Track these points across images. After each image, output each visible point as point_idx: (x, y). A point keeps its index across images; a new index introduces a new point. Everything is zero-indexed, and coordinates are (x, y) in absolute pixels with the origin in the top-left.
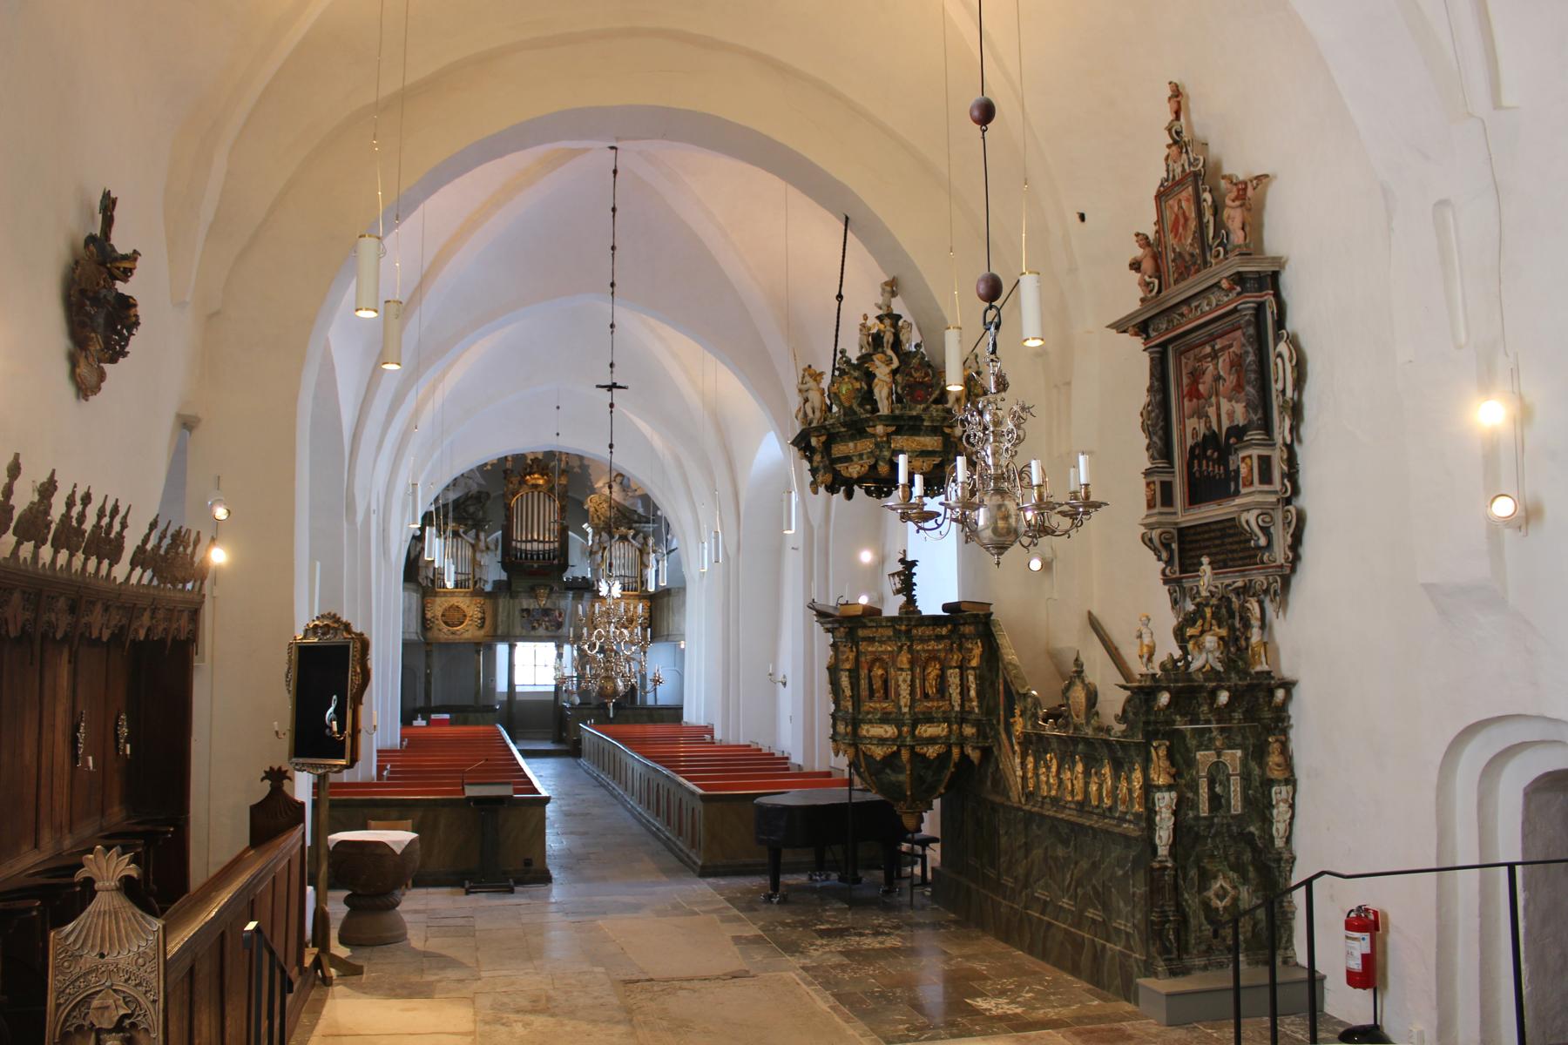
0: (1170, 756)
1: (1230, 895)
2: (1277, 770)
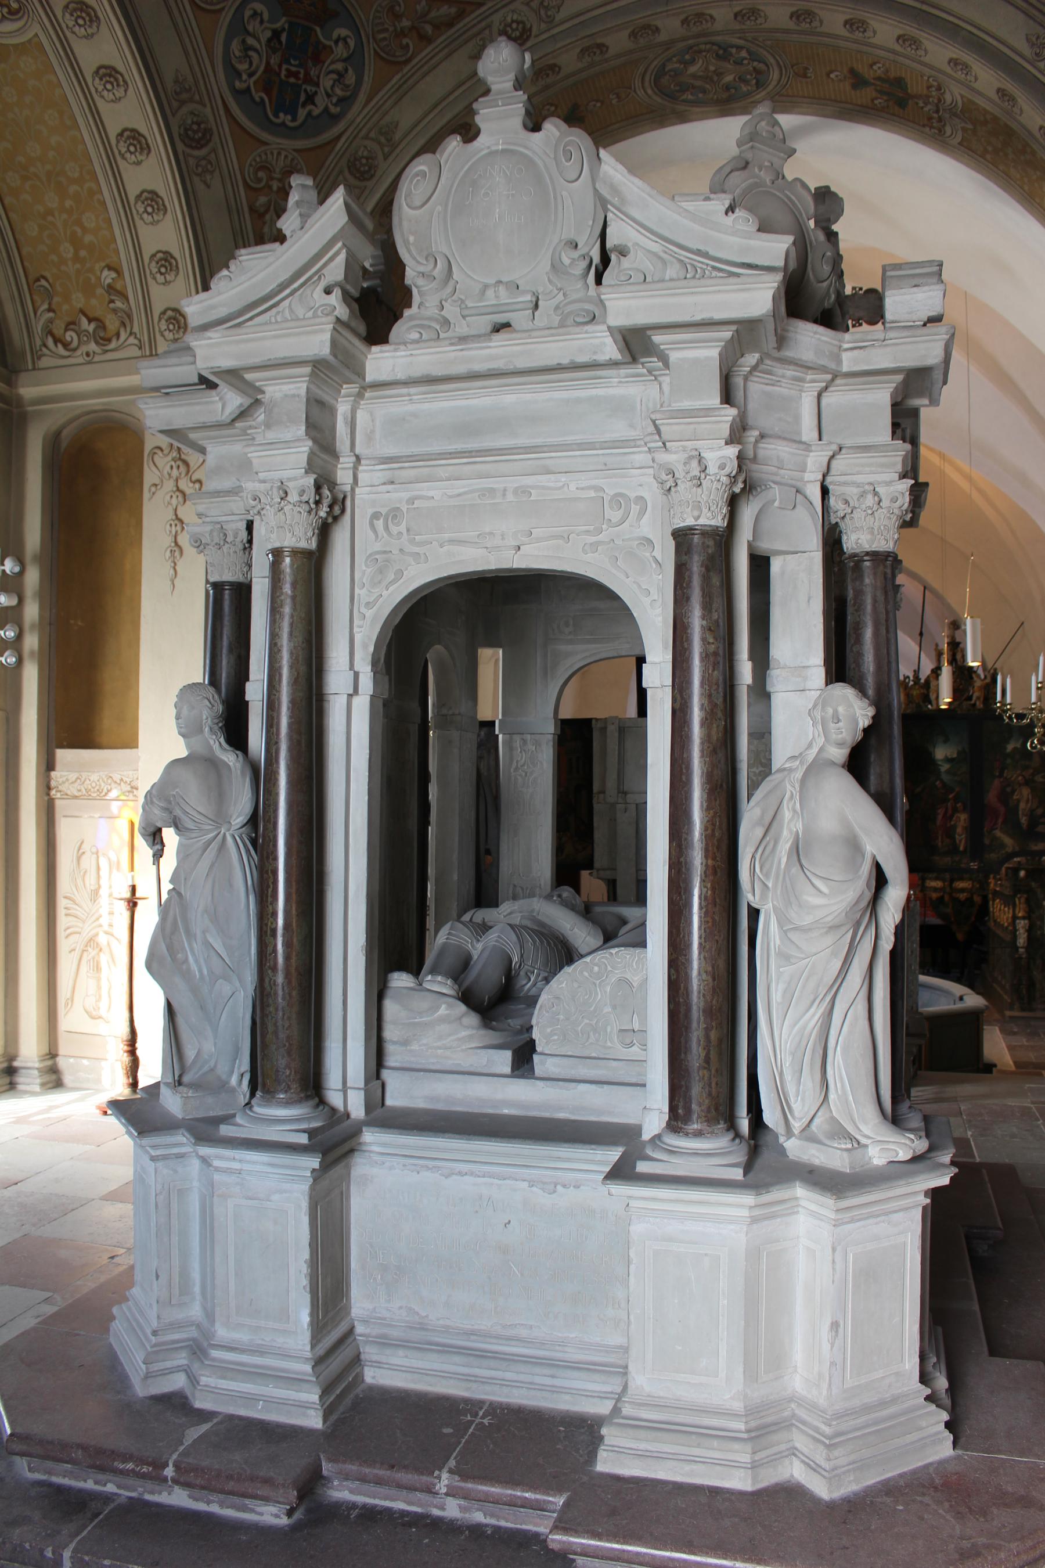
0: (1027, 901)
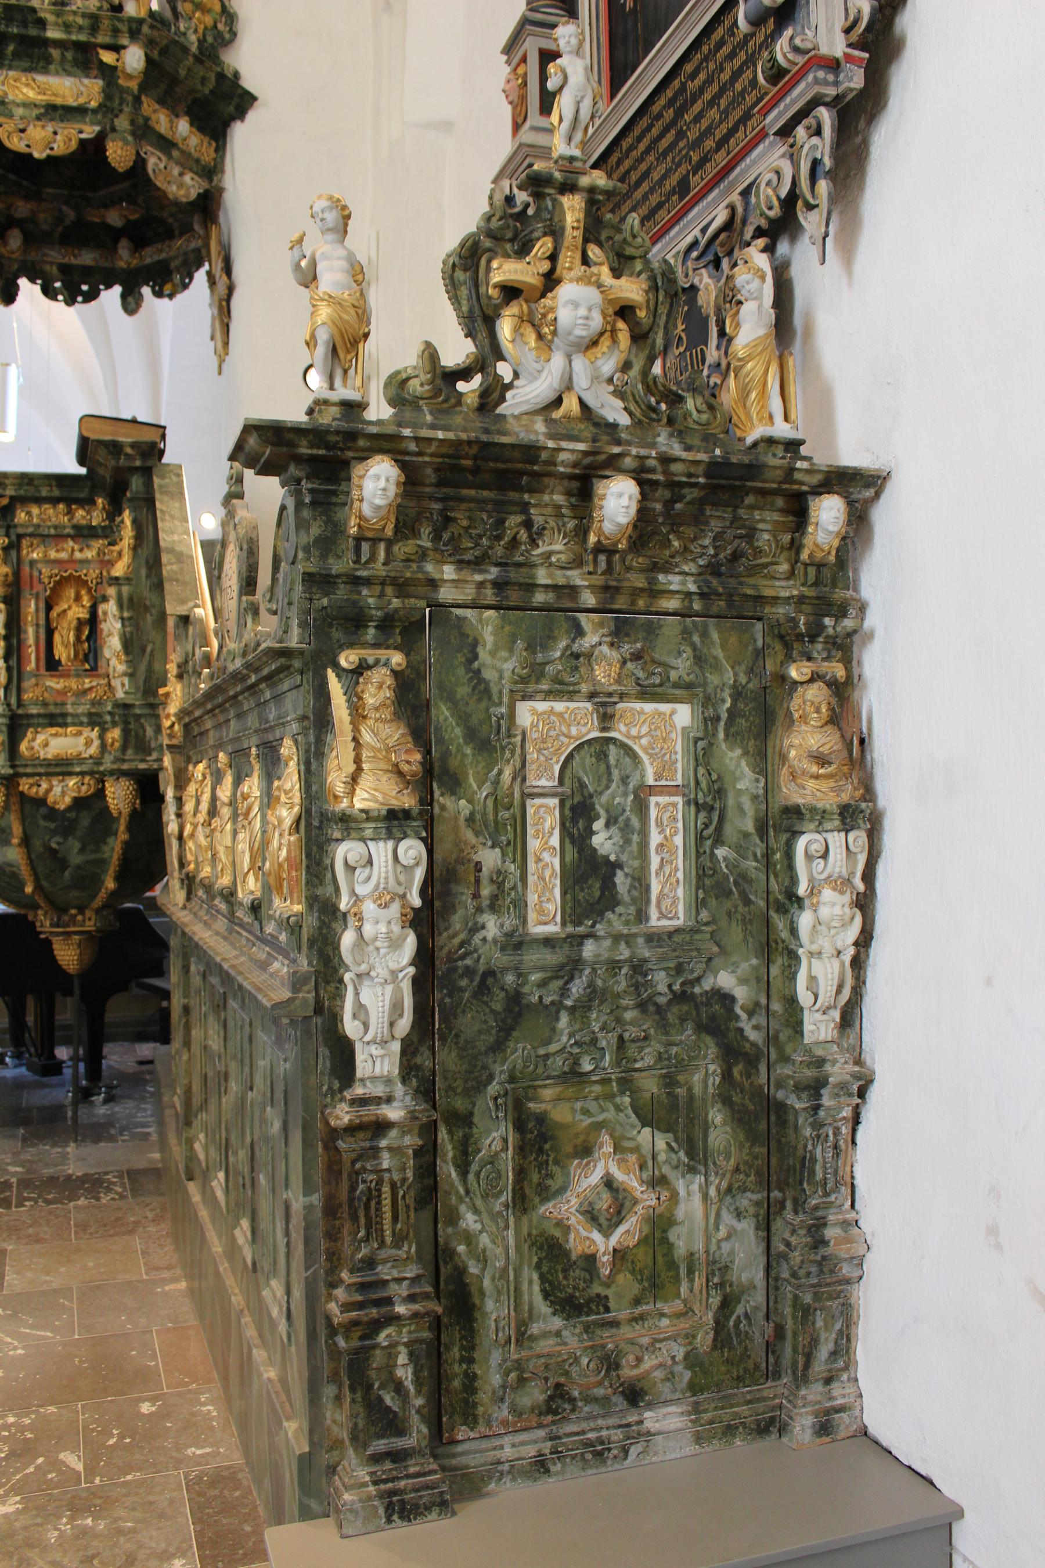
1: (639, 1209)
2: (817, 777)
